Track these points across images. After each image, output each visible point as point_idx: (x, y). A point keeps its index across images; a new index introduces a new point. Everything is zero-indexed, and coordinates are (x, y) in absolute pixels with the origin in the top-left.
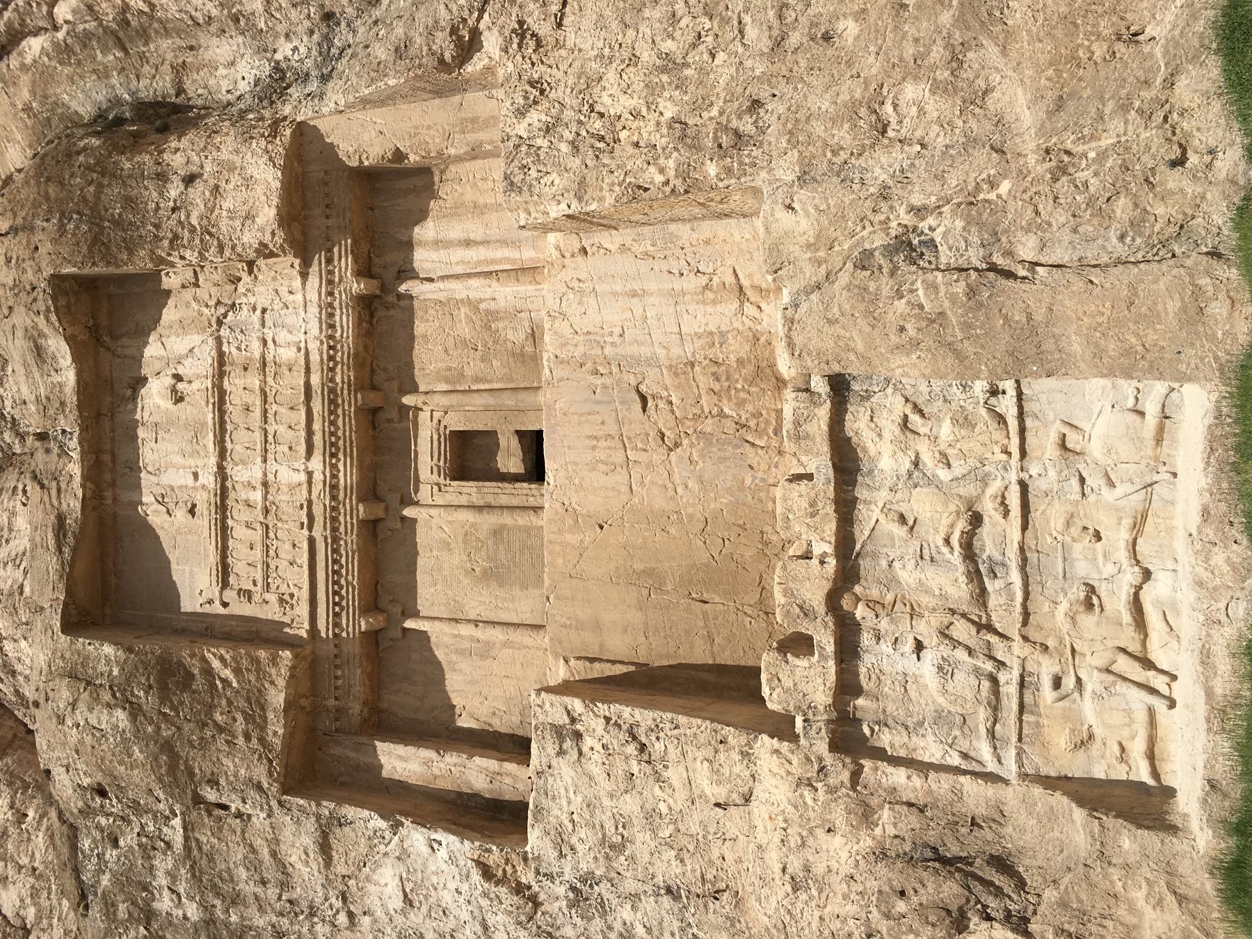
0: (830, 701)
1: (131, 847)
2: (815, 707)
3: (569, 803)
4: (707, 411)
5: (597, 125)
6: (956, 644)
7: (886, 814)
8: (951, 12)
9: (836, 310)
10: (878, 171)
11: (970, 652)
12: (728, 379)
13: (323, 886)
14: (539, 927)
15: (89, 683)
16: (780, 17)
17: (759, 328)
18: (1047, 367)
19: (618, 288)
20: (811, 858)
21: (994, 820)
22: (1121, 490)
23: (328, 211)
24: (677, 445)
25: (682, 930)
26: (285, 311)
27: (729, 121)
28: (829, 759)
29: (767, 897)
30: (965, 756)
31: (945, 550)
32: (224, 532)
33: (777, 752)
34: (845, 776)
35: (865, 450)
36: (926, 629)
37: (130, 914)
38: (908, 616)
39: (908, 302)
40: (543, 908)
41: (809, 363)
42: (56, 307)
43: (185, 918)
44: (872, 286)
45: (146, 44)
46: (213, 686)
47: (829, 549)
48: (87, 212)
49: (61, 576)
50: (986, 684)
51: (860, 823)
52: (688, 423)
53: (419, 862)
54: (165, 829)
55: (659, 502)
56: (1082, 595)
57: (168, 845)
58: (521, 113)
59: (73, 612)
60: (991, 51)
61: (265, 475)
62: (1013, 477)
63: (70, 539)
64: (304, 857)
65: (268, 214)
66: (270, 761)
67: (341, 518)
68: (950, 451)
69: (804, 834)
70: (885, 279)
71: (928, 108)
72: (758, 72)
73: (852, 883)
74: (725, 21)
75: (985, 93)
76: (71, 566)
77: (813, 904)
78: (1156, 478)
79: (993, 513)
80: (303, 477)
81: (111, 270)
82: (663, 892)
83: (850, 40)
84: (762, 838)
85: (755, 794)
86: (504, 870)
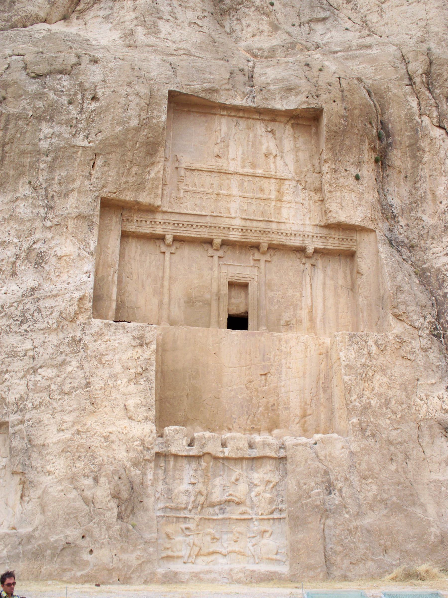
0: (173, 453)
3: (114, 340)
4: (260, 401)
5: (370, 374)
6: (196, 496)
7: (138, 472)
9: (311, 462)
11: (194, 501)
12: (272, 410)
13: (62, 215)
14: (61, 322)
15: (148, 105)
16: (398, 443)
17: (291, 423)
22: (252, 548)
24: (247, 388)
25: (74, 388)
29: (98, 425)
30: (158, 498)
31: (227, 494)
33: (152, 432)
34: (148, 457)
36: (200, 487)
37: (38, 108)
41: (291, 451)
42: (310, 108)
43: (40, 140)
44: (319, 475)
45: (410, 157)
46: (148, 166)
47: (226, 454)
49: (193, 92)
50: (183, 506)
52: (256, 393)
53: (79, 265)
54: (82, 136)
56: (217, 537)
58: (376, 342)
60: (385, 512)
61: (234, 196)
62: (254, 516)
63: (208, 96)
66: (115, 193)
67: (215, 231)
68: (261, 497)
70: (321, 479)
71: (370, 493)
72: (383, 435)
74: (399, 423)
76: (197, 96)
78: (256, 558)
80: (233, 215)
82: (88, 380)
83: (390, 467)
84: (118, 423)
85: (133, 421)
86: (82, 308)
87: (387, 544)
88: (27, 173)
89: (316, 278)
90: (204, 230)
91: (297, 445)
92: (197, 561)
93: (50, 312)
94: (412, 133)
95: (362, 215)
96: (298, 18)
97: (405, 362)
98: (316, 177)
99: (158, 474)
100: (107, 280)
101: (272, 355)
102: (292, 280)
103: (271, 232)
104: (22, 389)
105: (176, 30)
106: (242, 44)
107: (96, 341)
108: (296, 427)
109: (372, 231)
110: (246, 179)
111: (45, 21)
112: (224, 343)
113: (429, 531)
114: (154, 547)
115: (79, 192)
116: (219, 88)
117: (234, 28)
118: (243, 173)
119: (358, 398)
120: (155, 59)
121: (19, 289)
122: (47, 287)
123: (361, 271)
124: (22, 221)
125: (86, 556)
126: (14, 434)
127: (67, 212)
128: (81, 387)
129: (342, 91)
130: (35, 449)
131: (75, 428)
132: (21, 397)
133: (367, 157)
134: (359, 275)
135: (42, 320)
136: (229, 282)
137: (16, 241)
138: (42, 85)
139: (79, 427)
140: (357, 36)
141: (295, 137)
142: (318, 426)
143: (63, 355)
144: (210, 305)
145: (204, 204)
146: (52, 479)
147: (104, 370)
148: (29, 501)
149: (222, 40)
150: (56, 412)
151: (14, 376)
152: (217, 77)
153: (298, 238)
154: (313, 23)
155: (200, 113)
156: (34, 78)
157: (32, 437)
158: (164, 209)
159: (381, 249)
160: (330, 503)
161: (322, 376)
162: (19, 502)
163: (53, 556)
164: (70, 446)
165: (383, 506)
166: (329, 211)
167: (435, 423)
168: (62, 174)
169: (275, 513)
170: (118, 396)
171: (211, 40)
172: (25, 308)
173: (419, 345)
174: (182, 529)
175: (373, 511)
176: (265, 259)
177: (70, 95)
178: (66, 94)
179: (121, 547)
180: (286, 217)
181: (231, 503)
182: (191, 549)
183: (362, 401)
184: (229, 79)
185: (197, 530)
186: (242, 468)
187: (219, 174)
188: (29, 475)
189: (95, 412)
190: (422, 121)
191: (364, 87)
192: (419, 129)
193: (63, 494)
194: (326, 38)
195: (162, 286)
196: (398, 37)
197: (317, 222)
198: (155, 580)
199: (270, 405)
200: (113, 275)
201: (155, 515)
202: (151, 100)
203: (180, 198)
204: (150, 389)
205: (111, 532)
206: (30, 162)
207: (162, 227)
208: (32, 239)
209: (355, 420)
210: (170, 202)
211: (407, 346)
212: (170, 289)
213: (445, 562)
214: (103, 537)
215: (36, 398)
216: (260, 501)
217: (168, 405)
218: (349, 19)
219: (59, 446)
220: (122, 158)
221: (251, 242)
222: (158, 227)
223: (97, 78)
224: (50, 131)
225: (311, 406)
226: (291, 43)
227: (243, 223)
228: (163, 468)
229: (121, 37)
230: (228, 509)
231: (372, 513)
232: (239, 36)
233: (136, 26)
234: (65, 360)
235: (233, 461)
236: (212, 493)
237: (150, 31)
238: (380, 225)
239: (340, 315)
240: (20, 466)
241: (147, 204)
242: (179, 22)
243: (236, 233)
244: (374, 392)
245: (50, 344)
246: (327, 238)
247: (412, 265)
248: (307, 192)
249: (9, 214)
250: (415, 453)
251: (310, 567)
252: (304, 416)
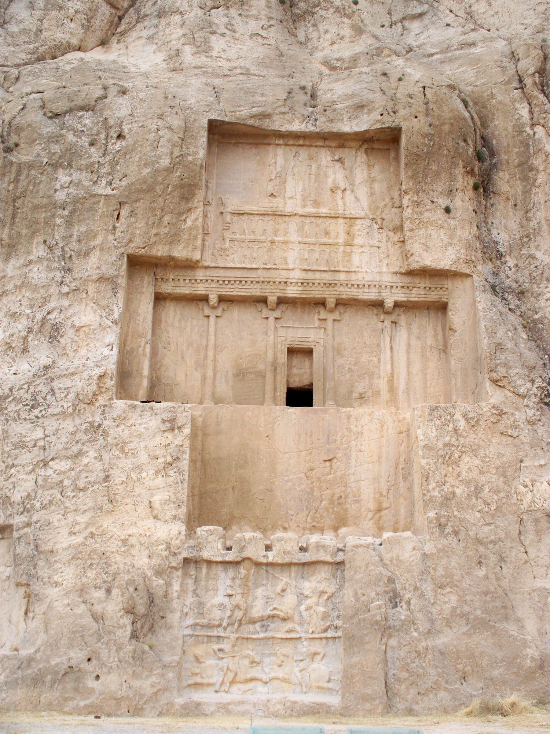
0: (205, 558)
3: (140, 424)
4: (324, 493)
5: (456, 456)
6: (233, 611)
7: (161, 582)
9: (372, 568)
11: (230, 617)
12: (338, 503)
13: (81, 278)
15: (183, 140)
16: (491, 542)
20: (137, 548)
22: (299, 674)
24: (307, 477)
25: (90, 482)
26: (378, 260)
27: (451, 521)
28: (181, 557)
29: (115, 527)
30: (187, 614)
31: (271, 608)
33: (180, 533)
34: (174, 564)
36: (238, 599)
37: (54, 153)
39: (374, 598)
41: (349, 554)
43: (56, 190)
44: (381, 584)
45: (520, 178)
46: (183, 213)
47: (270, 559)
49: (239, 119)
50: (217, 623)
52: (318, 484)
53: (100, 337)
54: (104, 182)
56: (256, 660)
58: (465, 416)
60: (465, 629)
61: (293, 243)
62: (303, 635)
63: (257, 123)
67: (268, 287)
68: (312, 611)
69: (146, 545)
71: (447, 606)
72: (470, 532)
74: (493, 516)
76: (243, 124)
78: (304, 687)
80: (291, 267)
81: (402, 165)
82: (106, 474)
83: (477, 573)
84: (140, 524)
85: (159, 521)
86: (102, 387)
87: (466, 669)
88: (42, 232)
89: (397, 339)
90: (255, 287)
91: (357, 546)
92: (231, 690)
93: (65, 394)
94: (522, 149)
95: (453, 256)
96: (388, 16)
97: (504, 439)
98: (395, 214)
99: (187, 584)
100: (138, 353)
101: (339, 436)
102: (368, 343)
103: (339, 285)
104: (29, 485)
105: (233, 45)
106: (319, 55)
107: (118, 426)
108: (369, 525)
109: (468, 276)
110: (308, 220)
111: (79, 49)
112: (278, 423)
113: (524, 653)
114: (174, 672)
115: (102, 250)
116: (272, 112)
117: (310, 37)
118: (304, 214)
119: (438, 486)
120: (196, 82)
121: (31, 368)
122: (63, 364)
123: (453, 327)
124: (35, 288)
125: (91, 683)
126: (19, 538)
127: (87, 274)
128: (99, 482)
129: (427, 103)
130: (42, 557)
131: (88, 531)
132: (29, 495)
133: (461, 183)
134: (451, 332)
135: (56, 404)
136: (288, 348)
137: (28, 311)
138: (60, 126)
139: (93, 529)
140: (459, 33)
141: (369, 165)
142: (397, 522)
143: (80, 445)
144: (264, 377)
145: (255, 255)
146: (59, 591)
147: (126, 461)
148: (33, 618)
149: (291, 52)
150: (68, 512)
151: (21, 471)
152: (271, 99)
153: (373, 290)
154: (408, 21)
155: (250, 144)
156: (51, 118)
157: (40, 542)
158: (206, 264)
159: (478, 299)
160: (395, 618)
161: (402, 459)
162: (23, 619)
163: (54, 681)
164: (81, 552)
165: (465, 621)
166: (410, 254)
167: (543, 515)
168: (81, 229)
169: (329, 631)
170: (142, 491)
171: (278, 53)
172: (37, 390)
173: (524, 417)
174: (214, 651)
175: (451, 628)
176: (333, 318)
177: (92, 135)
178: (88, 135)
179: (134, 672)
180: (358, 265)
181: (276, 618)
182: (225, 675)
183: (443, 490)
184: (285, 100)
185: (233, 652)
186: (290, 575)
187: (274, 217)
188: (34, 587)
189: (113, 511)
190: (534, 133)
191: (459, 96)
192: (531, 144)
193: (69, 608)
194: (422, 39)
195: (206, 357)
196: (510, 29)
197: (397, 269)
198: (172, 711)
199: (335, 498)
200: (144, 347)
201: (181, 633)
202: (186, 133)
203: (226, 249)
204: (182, 482)
205: (121, 654)
206: (44, 218)
207: (204, 285)
208: (46, 309)
209: (432, 514)
210: (213, 255)
211: (508, 419)
212: (215, 360)
213: (544, 693)
214: (112, 660)
215: (45, 496)
217: (209, 500)
218: (451, 11)
219: (69, 552)
220: (152, 205)
221: (314, 298)
222: (199, 285)
223: (124, 112)
224: (67, 179)
225: (388, 498)
226: (378, 48)
227: (303, 275)
228: (193, 577)
229: (164, 60)
230: (272, 626)
231: (449, 630)
232: (316, 45)
233: (183, 45)
234: (81, 450)
235: (279, 568)
236: (252, 607)
237: (200, 49)
238: (479, 268)
239: (429, 383)
240: (24, 576)
241: (184, 259)
242: (237, 35)
243: (295, 288)
244: (460, 479)
246: (410, 288)
247: (521, 316)
248: (384, 233)
249: (21, 280)
250: (513, 554)
251: (366, 698)
252: (379, 510)
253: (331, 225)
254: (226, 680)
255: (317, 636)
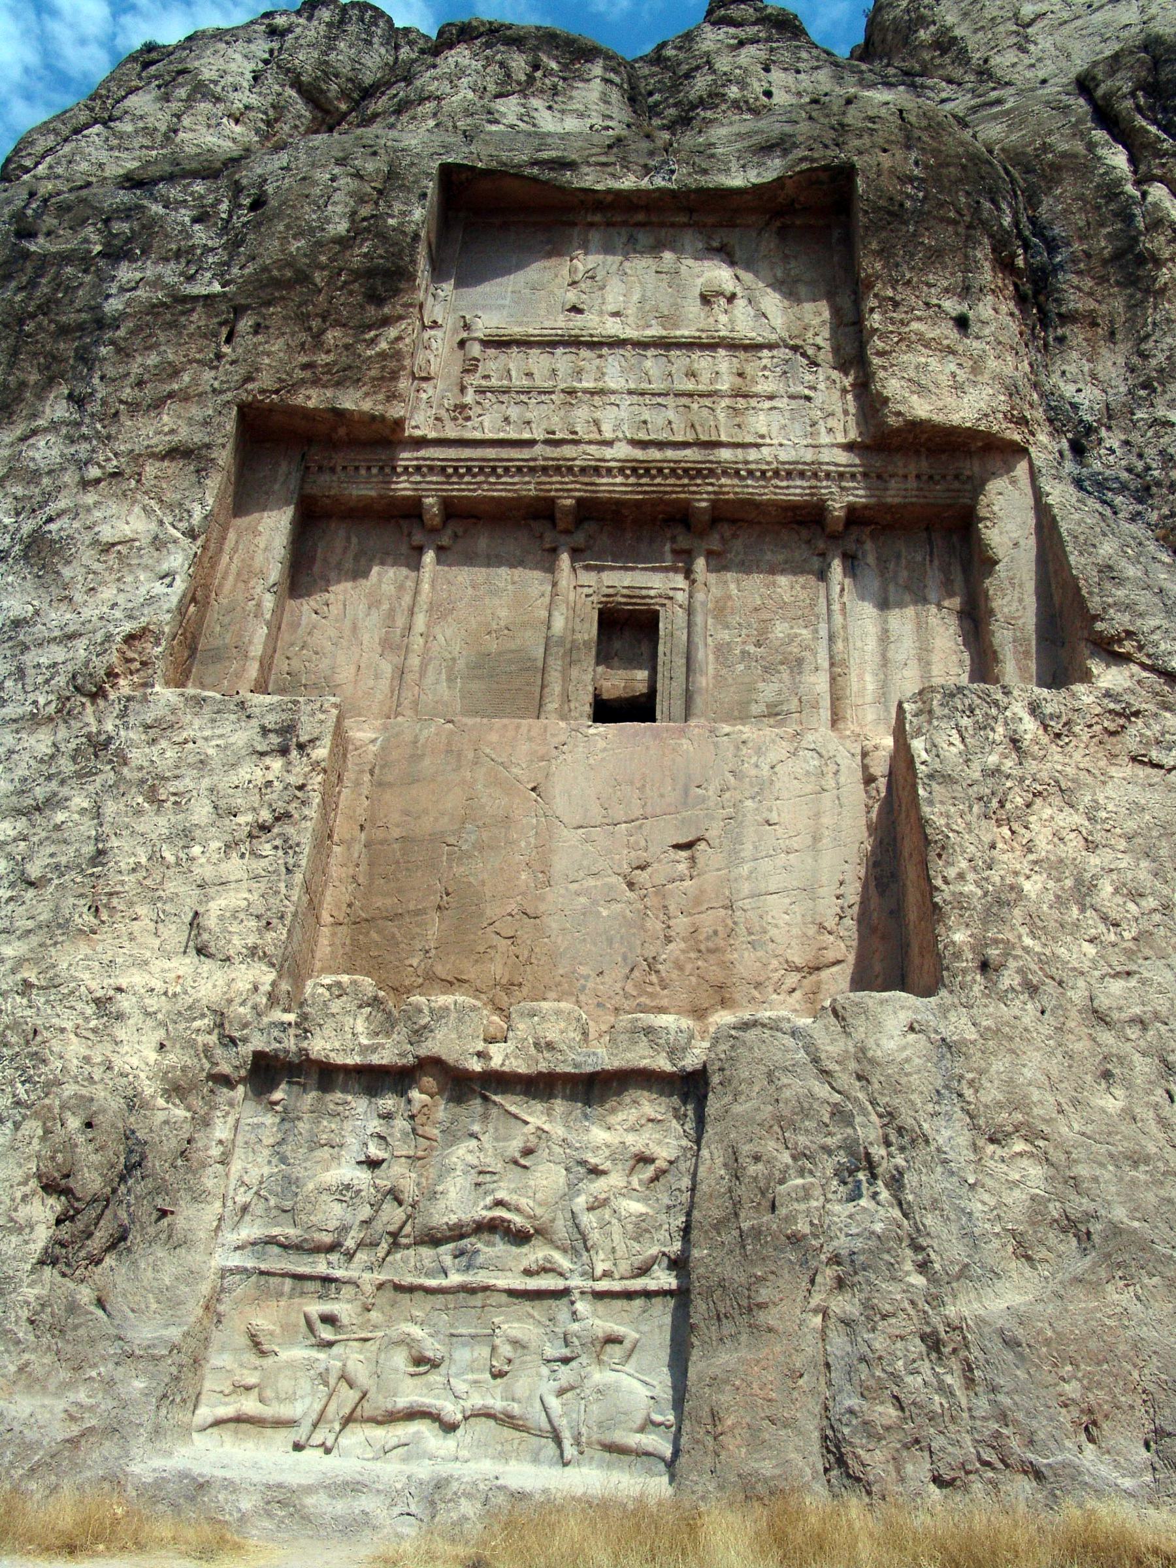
0: (313, 1056)
1: (191, 237)
2: (306, 1038)
3: (206, 739)
5: (1019, 801)
7: (180, 1113)
8: (1125, 1220)
10: (946, 1133)
11: (366, 1223)
14: (68, 699)
15: (380, 192)
18: (702, 1324)
19: (826, 820)
20: (131, 1022)
21: (170, 1237)
23: (925, 478)
24: (631, 885)
25: (57, 866)
27: (1016, 957)
28: (247, 1050)
29: (88, 968)
30: (245, 1209)
31: (489, 1200)
32: (549, 344)
33: (256, 989)
34: (225, 1068)
35: (613, 1111)
37: (117, 235)
38: (411, 1153)
39: (787, 1166)
40: (88, 704)
43: (108, 296)
45: (1118, 284)
46: (370, 328)
47: (496, 1063)
48: (926, 207)
49: (505, 164)
50: (327, 1238)
51: (168, 1081)
54: (208, 275)
55: (560, 864)
56: (429, 1354)
57: (190, 279)
58: (1034, 709)
59: (463, 176)
62: (576, 1282)
63: (547, 175)
64: (166, 429)
65: (921, 408)
66: (277, 392)
68: (607, 1213)
69: (159, 1016)
71: (1017, 1193)
73: (103, 1068)
75: (1029, 1258)
76: (516, 176)
77: (80, 1021)
78: (567, 1443)
79: (532, 1258)
80: (608, 435)
82: (100, 846)
83: (1102, 1103)
84: (158, 965)
85: (207, 961)
94: (1119, 226)
97: (1142, 772)
107: (154, 741)
114: (152, 1377)
124: (34, 476)
128: (79, 865)
131: (19, 977)
139: (31, 975)
143: (54, 785)
145: (529, 416)
168: (149, 362)
182: (330, 1396)
185: (362, 1327)
206: (76, 350)
216: (604, 1225)
222: (402, 479)
231: (1027, 1271)
245: (26, 756)
253: (702, 362)
254: (332, 1408)
255: (617, 1286)
